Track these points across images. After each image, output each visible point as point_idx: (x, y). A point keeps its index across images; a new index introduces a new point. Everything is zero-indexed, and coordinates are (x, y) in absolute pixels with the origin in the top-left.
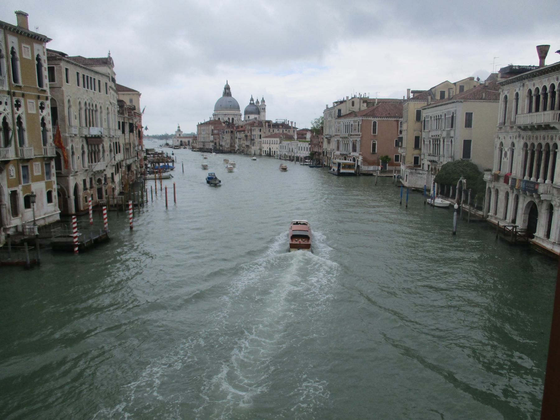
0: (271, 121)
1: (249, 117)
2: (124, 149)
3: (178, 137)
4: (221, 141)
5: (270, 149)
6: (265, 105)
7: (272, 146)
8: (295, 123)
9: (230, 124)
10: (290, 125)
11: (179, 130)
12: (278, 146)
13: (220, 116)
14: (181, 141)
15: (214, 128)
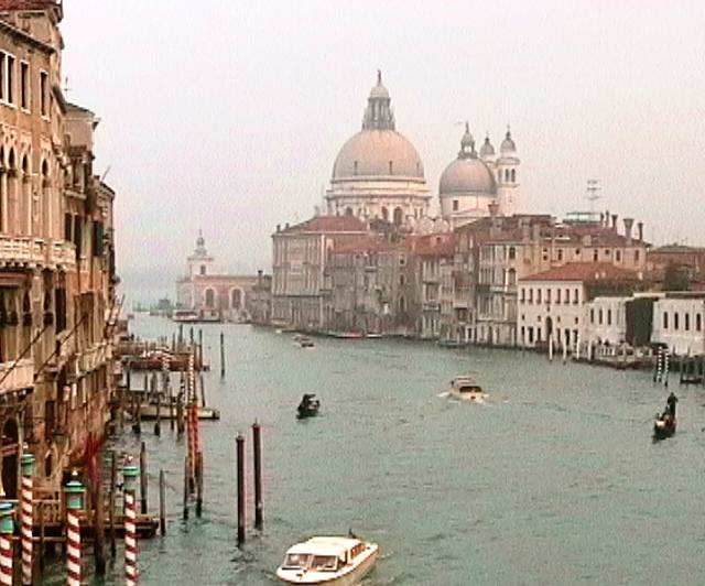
0: (549, 216)
1: (456, 202)
2: (76, 315)
3: (198, 278)
4: (360, 294)
5: (549, 320)
6: (517, 161)
7: (555, 311)
8: (640, 225)
9: (390, 230)
10: (621, 230)
11: (201, 253)
12: (581, 311)
13: (354, 200)
14: (210, 293)
15: (335, 244)
